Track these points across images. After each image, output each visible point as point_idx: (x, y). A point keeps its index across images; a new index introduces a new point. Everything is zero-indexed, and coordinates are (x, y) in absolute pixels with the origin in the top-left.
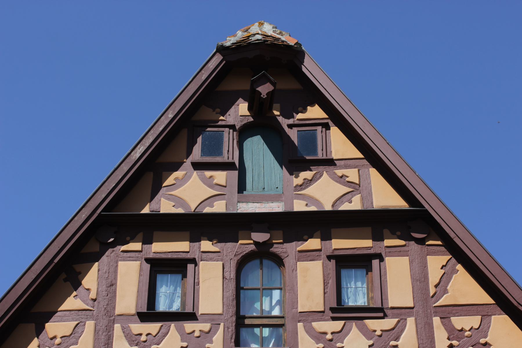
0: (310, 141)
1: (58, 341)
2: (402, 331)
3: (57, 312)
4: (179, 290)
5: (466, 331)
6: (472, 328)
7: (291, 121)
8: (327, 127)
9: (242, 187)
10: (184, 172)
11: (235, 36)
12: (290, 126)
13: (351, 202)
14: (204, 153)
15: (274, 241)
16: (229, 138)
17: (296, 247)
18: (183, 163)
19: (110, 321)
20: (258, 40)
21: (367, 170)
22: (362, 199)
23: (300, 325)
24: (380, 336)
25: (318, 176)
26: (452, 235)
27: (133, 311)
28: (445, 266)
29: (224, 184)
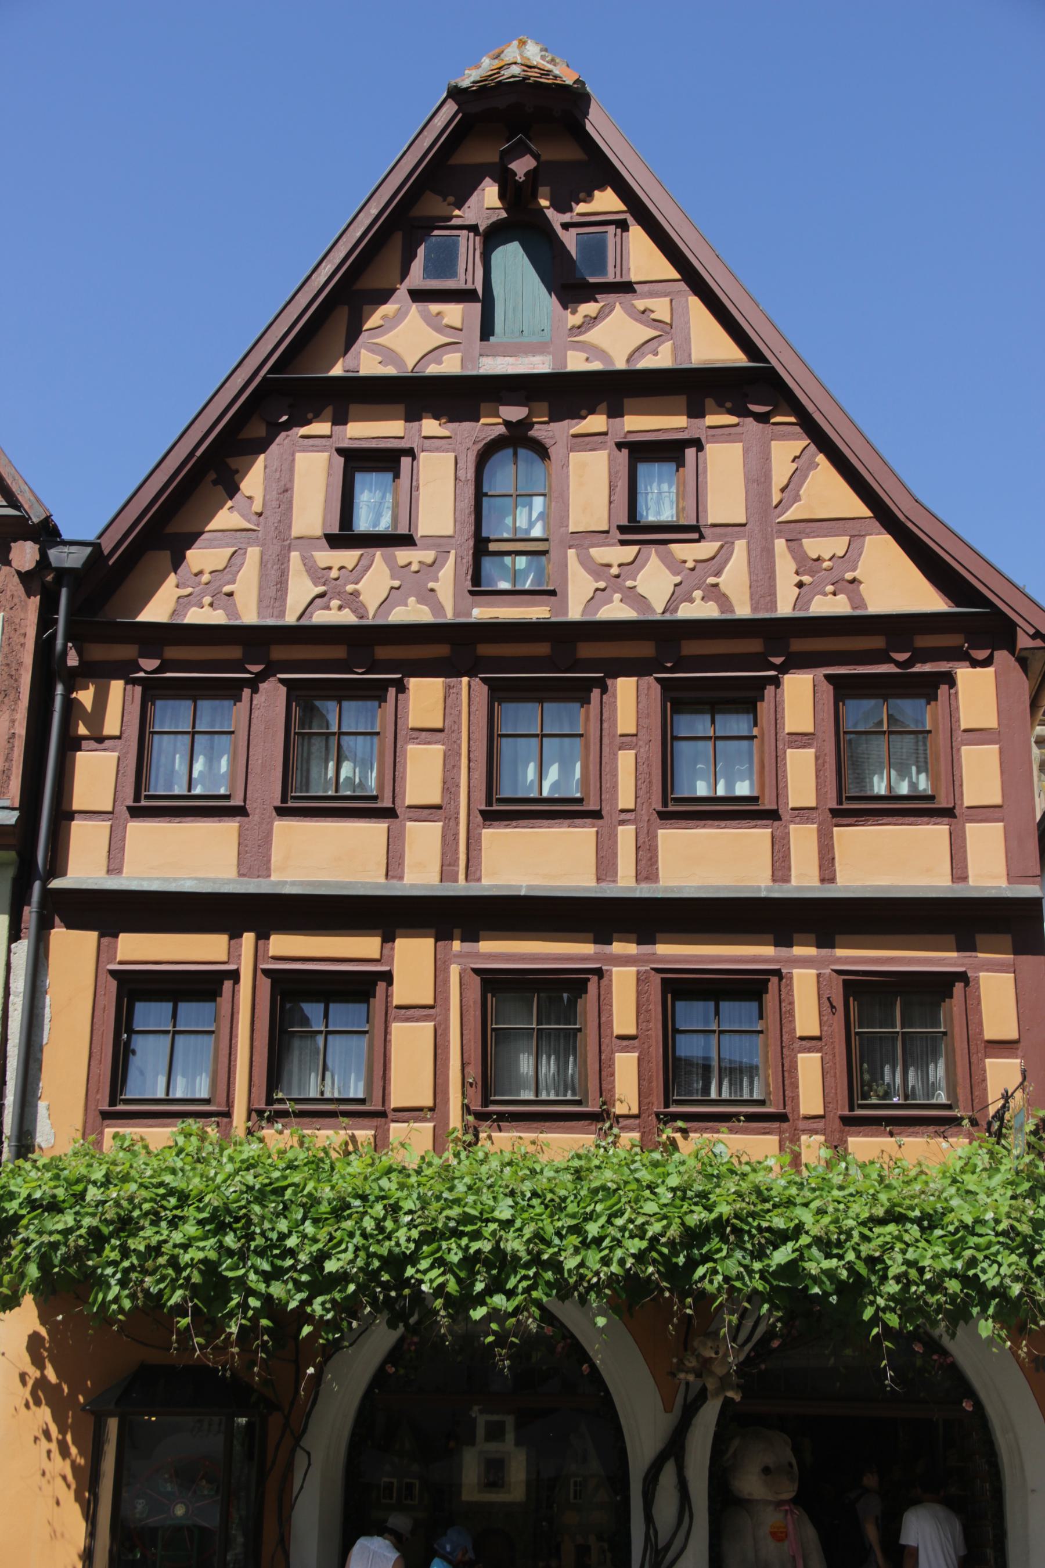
0: (596, 251)
1: (206, 578)
3: (203, 533)
4: (389, 498)
5: (825, 561)
6: (834, 556)
7: (566, 218)
8: (623, 226)
9: (487, 330)
10: (397, 306)
11: (478, 67)
12: (566, 226)
13: (656, 354)
14: (430, 272)
15: (535, 420)
16: (468, 247)
18: (395, 290)
19: (283, 548)
20: (513, 76)
21: (684, 299)
22: (675, 349)
23: (571, 552)
24: (693, 569)
25: (607, 311)
26: (811, 408)
27: (319, 532)
29: (459, 326)
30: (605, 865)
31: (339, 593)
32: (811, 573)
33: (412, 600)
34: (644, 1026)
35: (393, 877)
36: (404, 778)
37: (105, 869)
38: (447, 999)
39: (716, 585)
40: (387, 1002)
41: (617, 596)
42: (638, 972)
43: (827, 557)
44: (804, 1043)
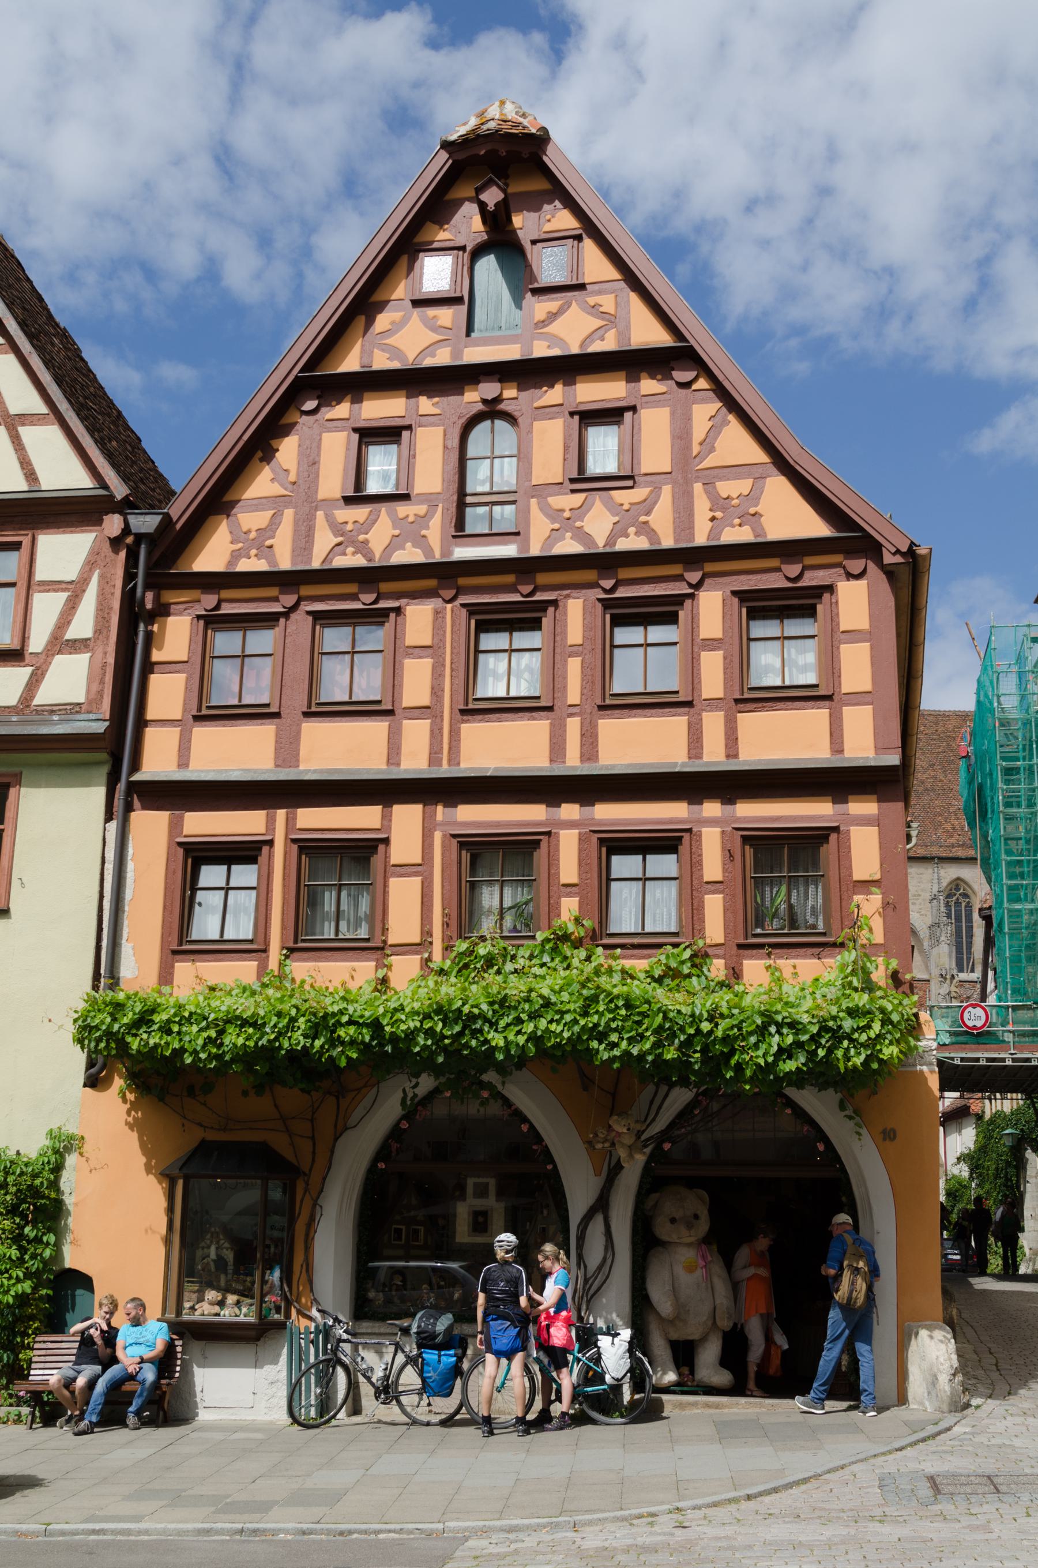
1: (253, 535)
2: (656, 502)
8: (579, 238)
13: (603, 340)
17: (533, 402)
22: (619, 334)
24: (628, 511)
27: (338, 495)
28: (712, 417)
30: (557, 748)
31: (353, 542)
32: (724, 510)
33: (409, 545)
34: (584, 876)
35: (392, 764)
36: (401, 686)
37: (176, 764)
38: (432, 858)
39: (646, 523)
40: (386, 862)
41: (568, 535)
42: (580, 834)
43: (735, 496)
44: (709, 886)
